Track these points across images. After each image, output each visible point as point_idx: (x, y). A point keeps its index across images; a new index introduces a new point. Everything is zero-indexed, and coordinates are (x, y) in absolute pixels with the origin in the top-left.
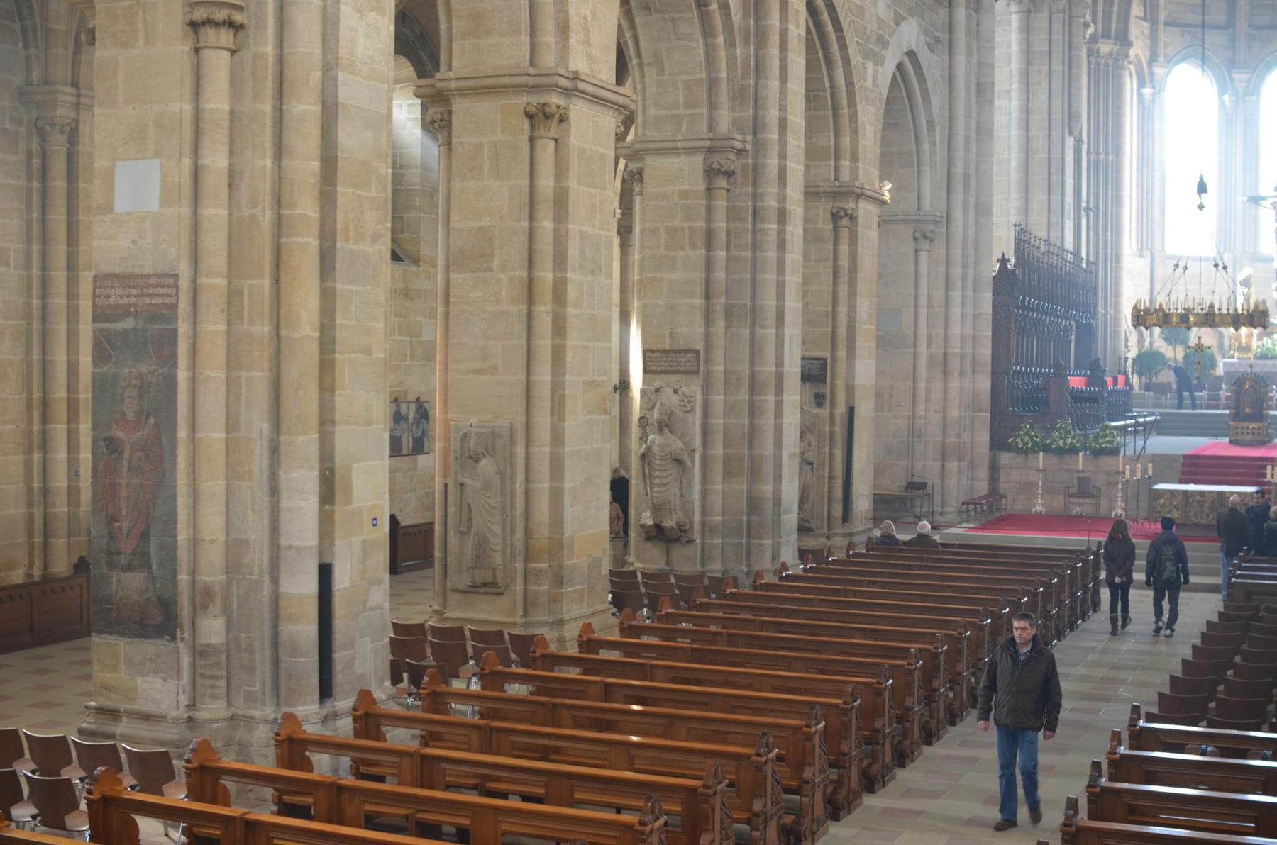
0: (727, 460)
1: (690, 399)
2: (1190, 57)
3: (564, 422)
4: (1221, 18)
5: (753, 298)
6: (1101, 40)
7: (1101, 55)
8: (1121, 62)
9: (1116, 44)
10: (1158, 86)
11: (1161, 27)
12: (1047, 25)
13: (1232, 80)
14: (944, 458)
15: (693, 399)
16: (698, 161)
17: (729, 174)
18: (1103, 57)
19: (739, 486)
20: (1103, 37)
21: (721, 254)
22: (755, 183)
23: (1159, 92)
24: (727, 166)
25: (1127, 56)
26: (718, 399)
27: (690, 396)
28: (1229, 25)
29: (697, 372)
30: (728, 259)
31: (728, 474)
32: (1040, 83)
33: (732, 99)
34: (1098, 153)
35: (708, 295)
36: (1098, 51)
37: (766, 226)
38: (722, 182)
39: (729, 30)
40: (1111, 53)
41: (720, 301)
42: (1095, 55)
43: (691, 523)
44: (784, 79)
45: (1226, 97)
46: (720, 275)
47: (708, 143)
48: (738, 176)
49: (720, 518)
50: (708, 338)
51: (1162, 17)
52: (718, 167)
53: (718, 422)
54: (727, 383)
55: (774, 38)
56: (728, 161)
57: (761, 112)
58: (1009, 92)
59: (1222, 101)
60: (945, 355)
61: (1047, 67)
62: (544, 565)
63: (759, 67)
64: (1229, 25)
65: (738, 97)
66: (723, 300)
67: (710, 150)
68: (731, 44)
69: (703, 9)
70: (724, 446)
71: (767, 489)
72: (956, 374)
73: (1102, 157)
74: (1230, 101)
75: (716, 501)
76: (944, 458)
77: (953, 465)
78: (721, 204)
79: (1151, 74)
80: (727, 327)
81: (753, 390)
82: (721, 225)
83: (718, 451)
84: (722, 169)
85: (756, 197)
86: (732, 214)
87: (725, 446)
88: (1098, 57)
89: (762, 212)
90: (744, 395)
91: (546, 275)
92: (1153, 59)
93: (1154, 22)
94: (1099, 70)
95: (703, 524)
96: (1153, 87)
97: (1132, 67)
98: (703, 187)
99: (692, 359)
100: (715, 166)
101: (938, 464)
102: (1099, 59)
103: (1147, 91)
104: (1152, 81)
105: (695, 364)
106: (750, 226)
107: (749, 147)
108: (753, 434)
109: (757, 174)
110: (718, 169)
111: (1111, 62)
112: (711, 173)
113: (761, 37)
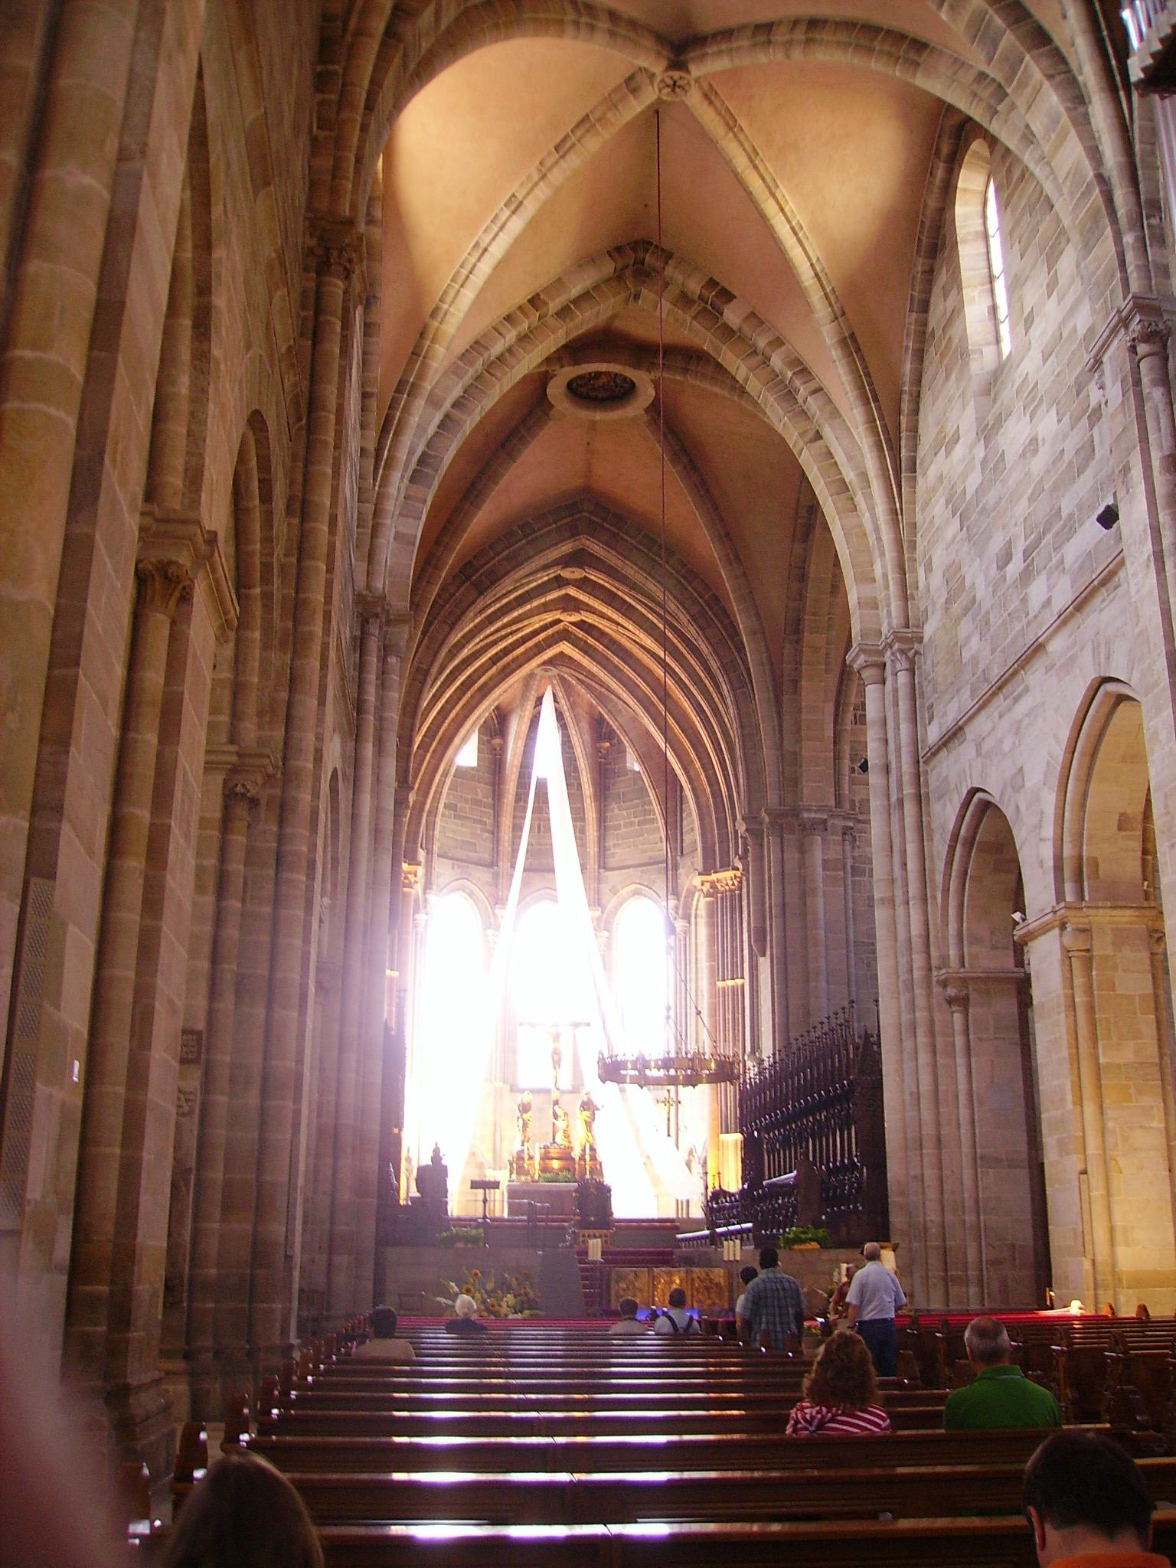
0: (228, 1185)
1: (187, 1096)
2: (458, 889)
3: (150, 1049)
4: (486, 856)
5: (272, 969)
11: (435, 856)
14: (331, 1251)
15: (191, 1097)
16: (220, 778)
17: (254, 802)
19: (243, 1226)
21: (234, 904)
22: (282, 821)
24: (253, 791)
26: (221, 1099)
27: (191, 1093)
28: (492, 864)
29: (196, 1061)
30: (243, 914)
31: (227, 1208)
33: (260, 714)
35: (215, 959)
37: (295, 876)
38: (241, 810)
39: (267, 628)
41: (229, 967)
43: (181, 1277)
44: (322, 703)
46: (231, 933)
47: (234, 759)
48: (263, 808)
49: (213, 1271)
50: (211, 1014)
51: (436, 848)
52: (243, 791)
53: (219, 1133)
54: (232, 1080)
55: (316, 648)
56: (252, 785)
57: (296, 735)
60: (336, 1127)
62: (104, 1289)
63: (294, 682)
64: (492, 864)
65: (266, 712)
66: (234, 967)
67: (234, 770)
68: (266, 646)
69: (243, 591)
70: (226, 1167)
71: (278, 1230)
72: (349, 1150)
75: (212, 1246)
76: (331, 1251)
77: (342, 1260)
78: (239, 839)
79: (425, 900)
80: (236, 1005)
81: (264, 1094)
82: (236, 867)
83: (217, 1175)
84: (249, 795)
85: (281, 839)
86: (251, 856)
87: (227, 1168)
89: (290, 858)
90: (253, 1098)
91: (141, 813)
92: (428, 886)
93: (429, 852)
95: (192, 1278)
98: (218, 815)
99: (191, 1043)
100: (239, 789)
101: (325, 1257)
103: (421, 917)
104: (425, 907)
105: (195, 1049)
106: (272, 873)
107: (279, 776)
108: (262, 1152)
109: (283, 811)
110: (243, 794)
112: (231, 797)
113: (297, 642)
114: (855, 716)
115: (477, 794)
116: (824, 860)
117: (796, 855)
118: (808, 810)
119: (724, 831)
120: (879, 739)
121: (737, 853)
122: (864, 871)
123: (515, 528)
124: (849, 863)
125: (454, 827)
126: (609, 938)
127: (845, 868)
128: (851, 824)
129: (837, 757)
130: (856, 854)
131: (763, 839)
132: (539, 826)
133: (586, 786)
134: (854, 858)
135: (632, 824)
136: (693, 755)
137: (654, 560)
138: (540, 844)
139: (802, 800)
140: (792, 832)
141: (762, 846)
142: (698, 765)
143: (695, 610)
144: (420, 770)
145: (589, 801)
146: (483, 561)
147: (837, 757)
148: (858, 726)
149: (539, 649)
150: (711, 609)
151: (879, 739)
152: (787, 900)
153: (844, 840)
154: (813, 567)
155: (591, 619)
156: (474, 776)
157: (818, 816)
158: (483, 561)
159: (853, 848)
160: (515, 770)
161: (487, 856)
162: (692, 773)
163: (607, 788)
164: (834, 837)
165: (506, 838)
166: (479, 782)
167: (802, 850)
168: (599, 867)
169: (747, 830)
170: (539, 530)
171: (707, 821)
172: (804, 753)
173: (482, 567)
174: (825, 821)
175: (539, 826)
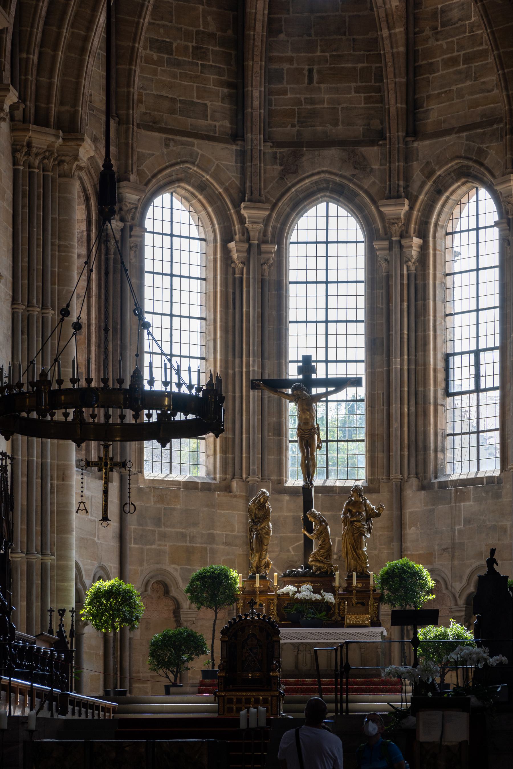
6: (32, 127)
7: (34, 150)
8: (66, 167)
9: (58, 137)
10: (129, 217)
13: (242, 220)
18: (37, 155)
20: (35, 124)
23: (131, 229)
25: (76, 158)
34: (30, 304)
36: (29, 145)
40: (50, 150)
42: (25, 149)
45: (232, 245)
59: (226, 252)
73: (36, 311)
74: (237, 251)
88: (28, 154)
94: (31, 174)
96: (122, 220)
97: (83, 174)
102: (31, 159)
111: (50, 163)
125: (166, 78)
126: (424, 248)
132: (310, 71)
135: (454, 61)
138: (312, 101)
161: (227, 123)
165: (256, 94)
168: (407, 135)
175: (310, 71)
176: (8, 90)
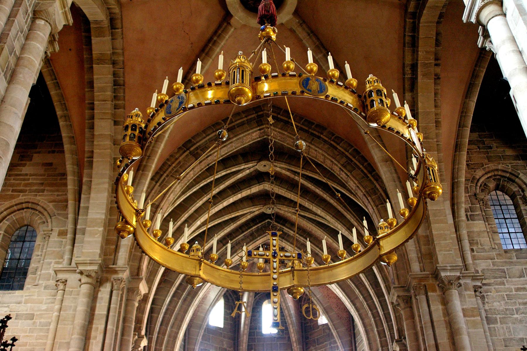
12: (108, 296)
32: (96, 337)
58: (68, 343)
61: (103, 326)
114: (467, 215)
115: (223, 345)
116: (463, 309)
117: (440, 307)
118: (445, 270)
119: (384, 339)
120: (513, 51)
121: (392, 338)
122: (496, 320)
123: (220, 121)
124: (484, 315)
127: (480, 315)
128: (479, 284)
129: (459, 240)
130: (487, 307)
131: (411, 303)
133: (293, 335)
134: (486, 310)
136: (357, 292)
137: (312, 134)
139: (438, 264)
140: (434, 291)
141: (411, 307)
142: (361, 298)
143: (344, 160)
144: (174, 310)
145: (295, 344)
146: (198, 140)
147: (459, 240)
148: (470, 222)
149: (253, 237)
150: (355, 157)
151: (513, 51)
152: (439, 341)
153: (476, 296)
154: (420, 105)
155: (284, 211)
156: (221, 333)
157: (453, 274)
158: (198, 140)
159: (484, 303)
160: (246, 327)
162: (358, 305)
163: (307, 338)
164: (469, 292)
166: (224, 337)
167: (445, 302)
169: (398, 296)
170: (236, 121)
171: (371, 335)
172: (434, 232)
173: (197, 142)
174: (459, 278)
176: (143, 337)
